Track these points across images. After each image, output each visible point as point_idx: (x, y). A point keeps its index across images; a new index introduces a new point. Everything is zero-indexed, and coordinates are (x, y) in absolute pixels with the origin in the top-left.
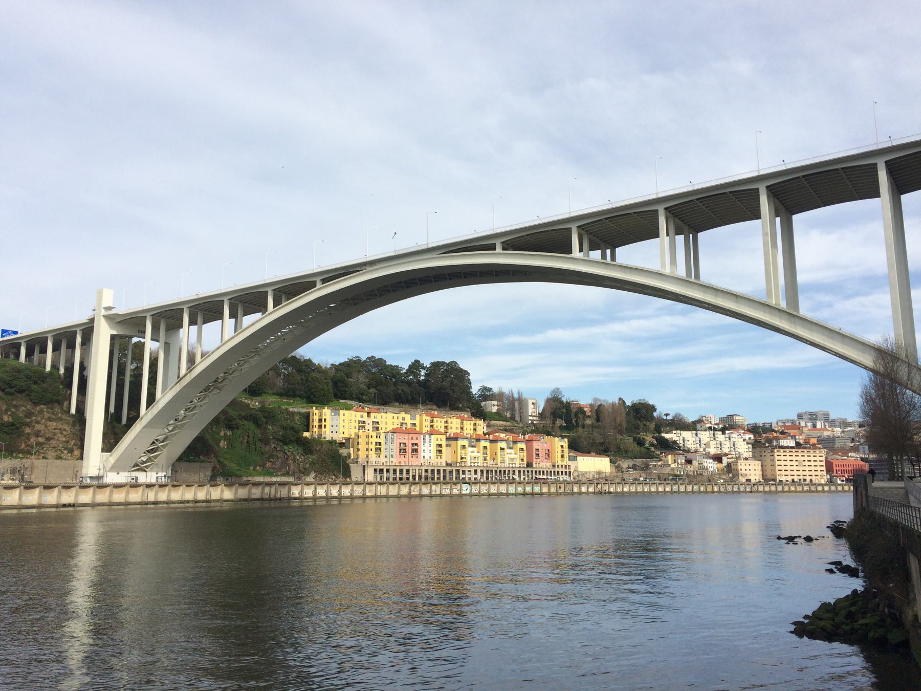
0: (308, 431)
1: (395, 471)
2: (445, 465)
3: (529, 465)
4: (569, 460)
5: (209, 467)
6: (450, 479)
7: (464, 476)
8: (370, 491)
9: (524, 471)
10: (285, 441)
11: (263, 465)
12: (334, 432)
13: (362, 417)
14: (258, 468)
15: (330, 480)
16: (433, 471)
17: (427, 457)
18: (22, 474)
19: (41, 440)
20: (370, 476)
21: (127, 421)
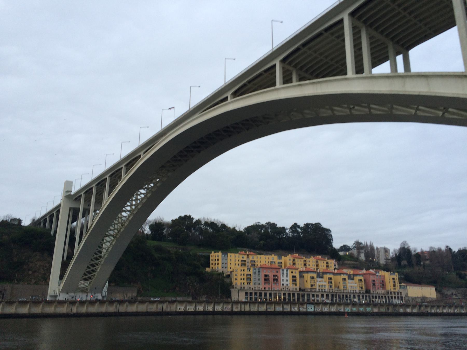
0: (209, 267)
1: (261, 294)
2: (299, 290)
3: (368, 291)
4: (401, 288)
6: (308, 300)
7: (313, 299)
8: (237, 308)
9: (363, 297)
12: (224, 268)
15: (216, 300)
16: (289, 295)
17: (285, 285)
18: (3, 293)
19: (30, 272)
21: (67, 258)
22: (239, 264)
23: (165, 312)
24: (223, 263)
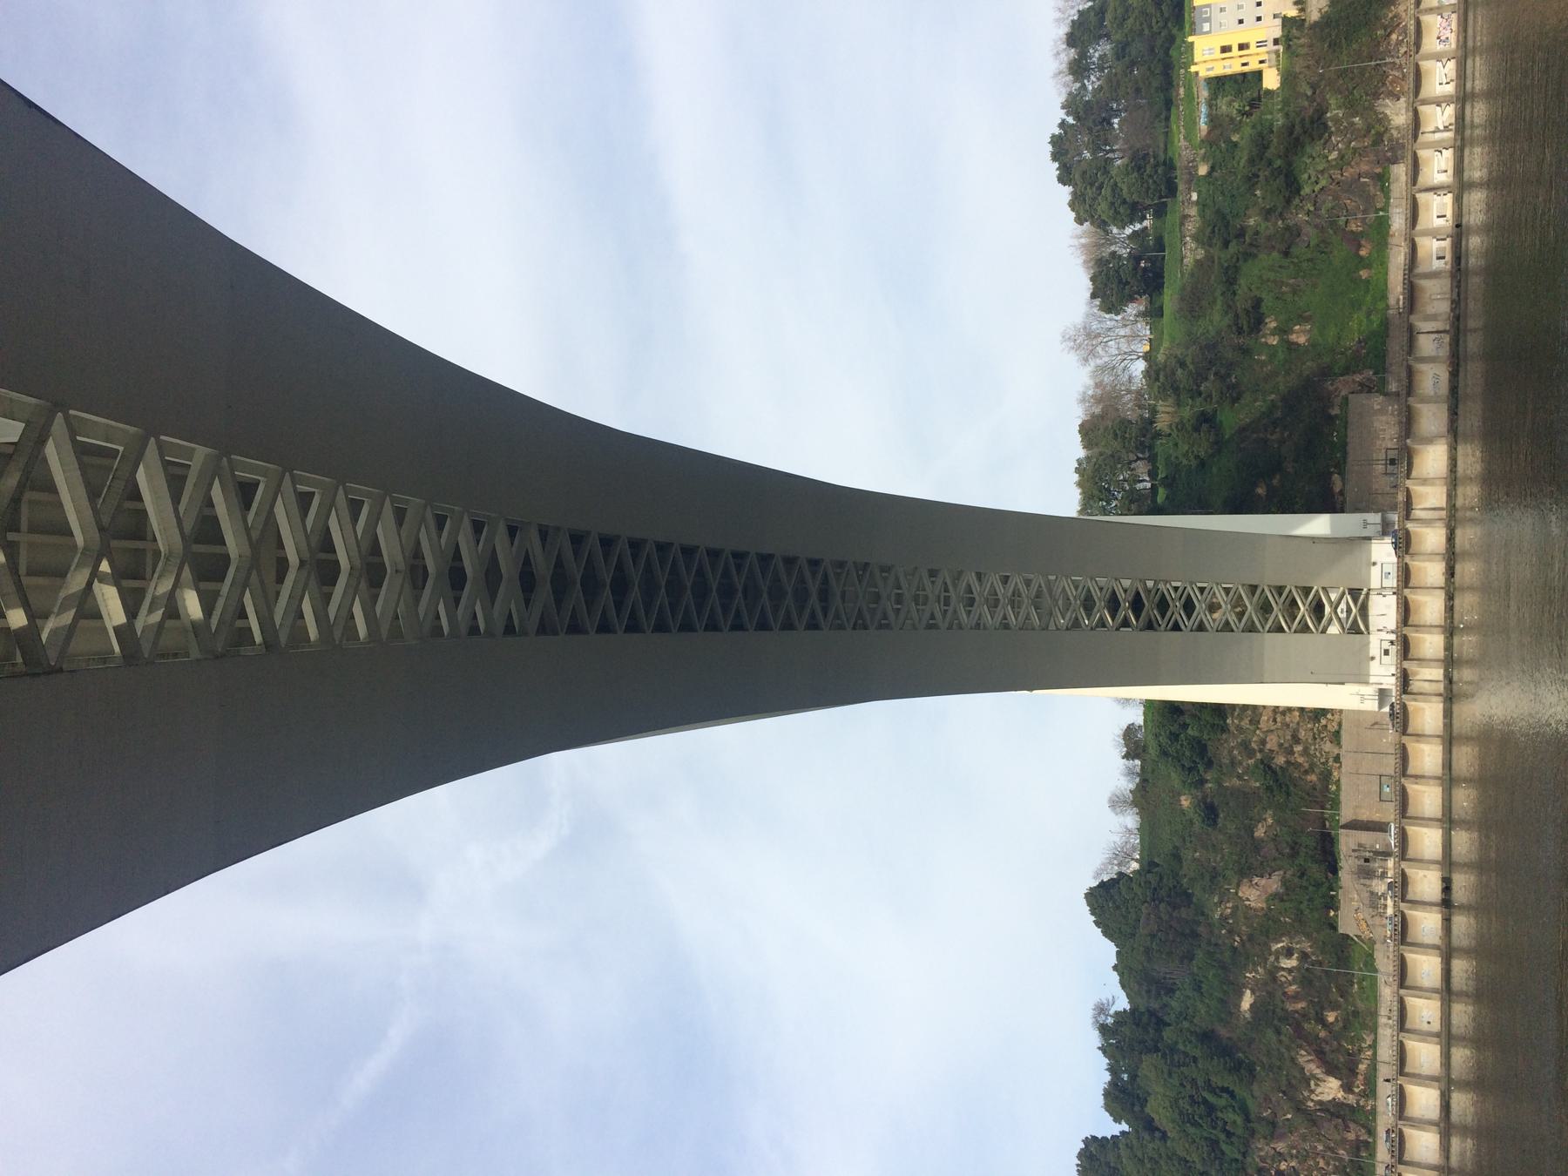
0: (1258, 75)
5: (1358, 401)
10: (1291, 186)
11: (1355, 240)
12: (1260, 11)
14: (1363, 253)
23: (1452, 325)
24: (1241, 22)
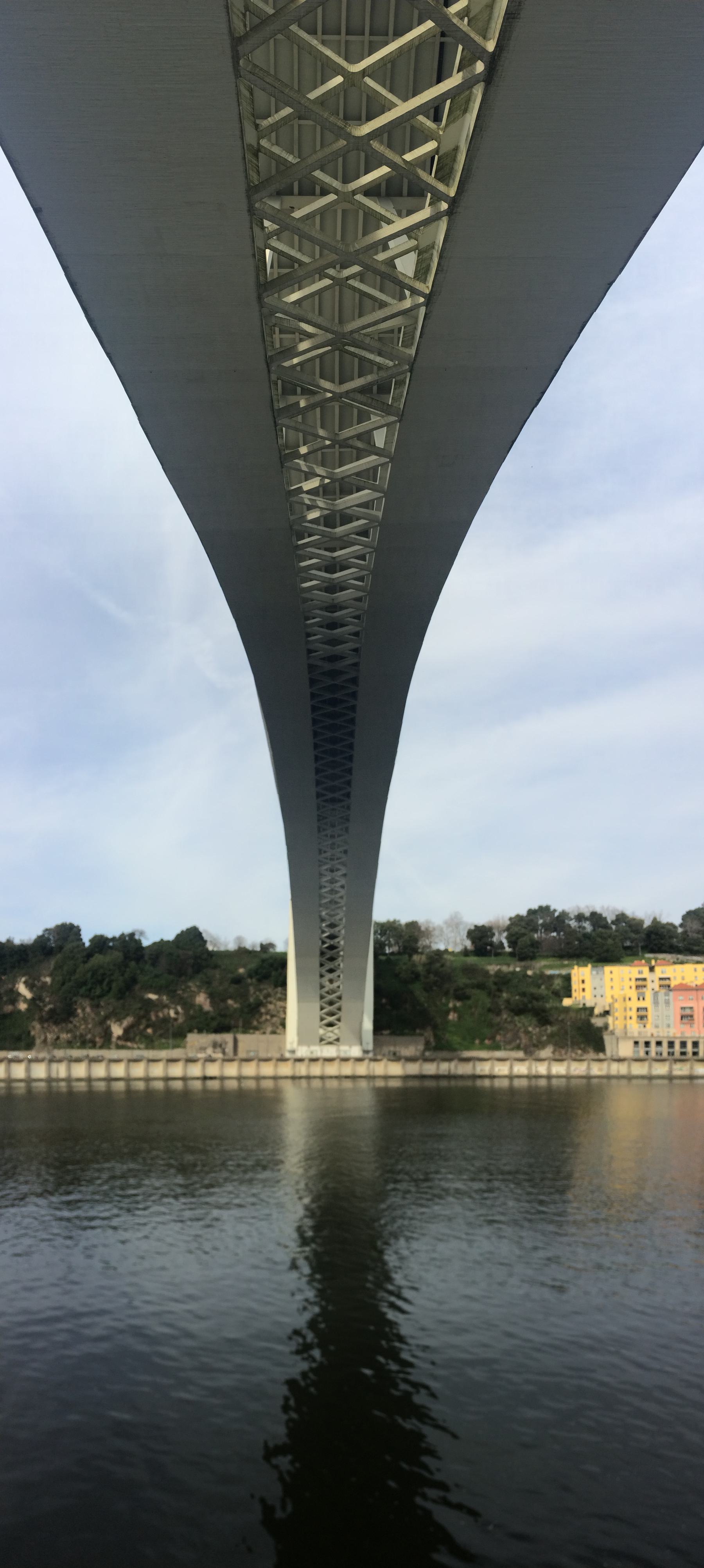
12: (599, 997)
13: (640, 972)
20: (626, 1049)
22: (631, 987)
